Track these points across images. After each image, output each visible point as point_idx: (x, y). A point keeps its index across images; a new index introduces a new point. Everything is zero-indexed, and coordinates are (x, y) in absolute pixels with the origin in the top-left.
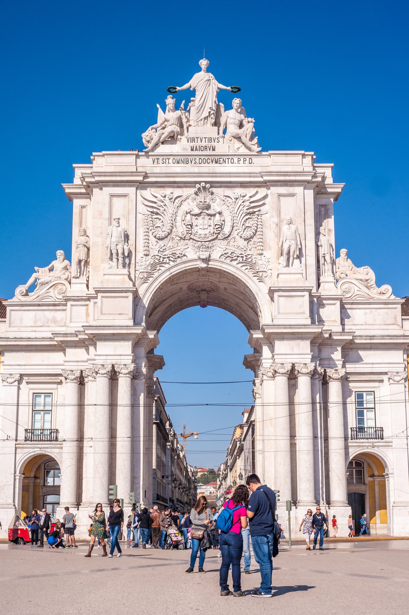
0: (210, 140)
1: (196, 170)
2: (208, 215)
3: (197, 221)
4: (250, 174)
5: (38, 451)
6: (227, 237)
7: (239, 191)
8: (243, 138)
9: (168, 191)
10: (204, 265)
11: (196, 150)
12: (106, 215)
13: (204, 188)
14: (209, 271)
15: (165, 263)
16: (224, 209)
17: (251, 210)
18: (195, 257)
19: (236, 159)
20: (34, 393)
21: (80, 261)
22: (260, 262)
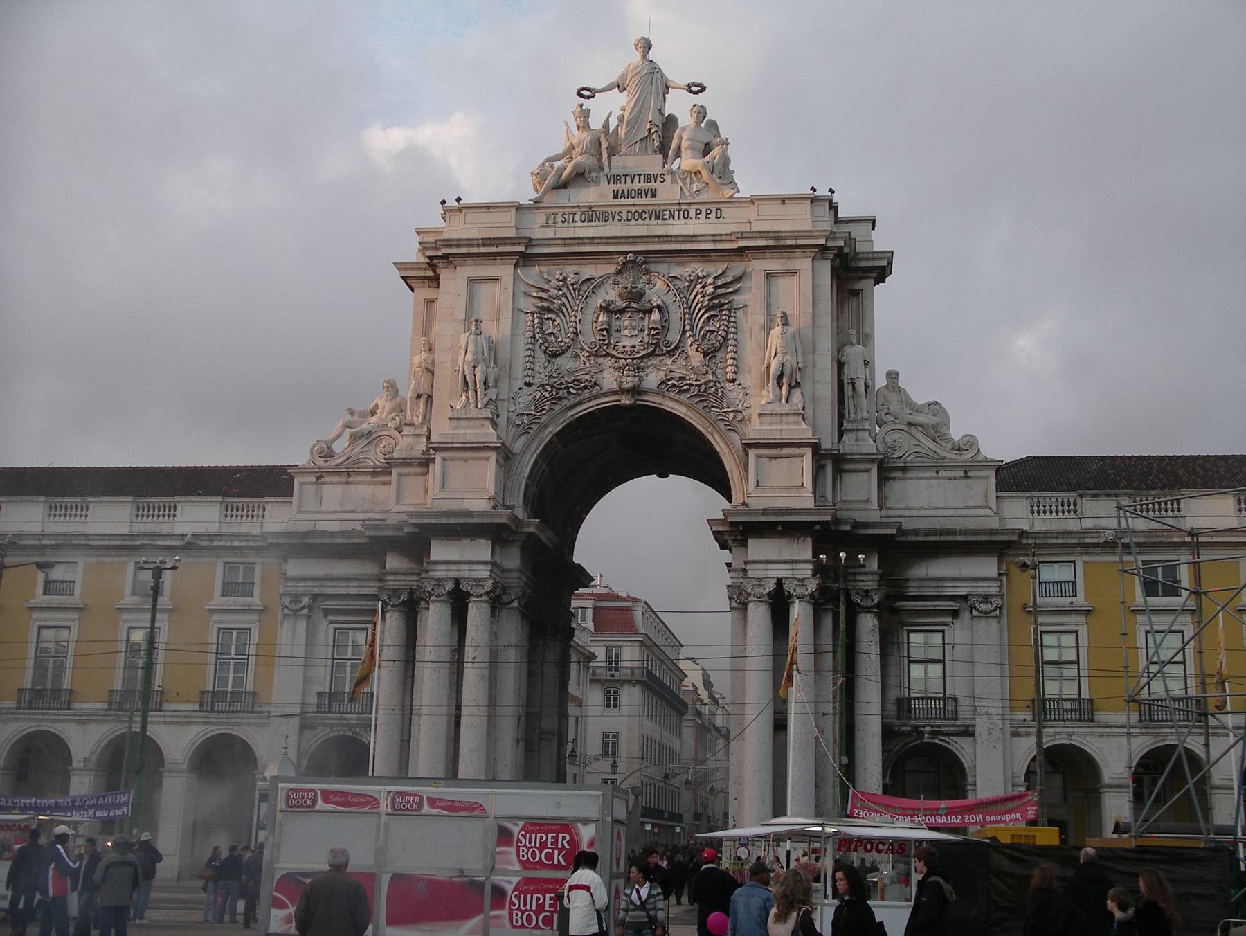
0: (648, 178)
2: (638, 311)
3: (618, 323)
4: (715, 237)
6: (673, 350)
7: (698, 268)
9: (570, 270)
10: (626, 401)
11: (623, 196)
13: (633, 262)
15: (560, 399)
16: (669, 299)
17: (716, 301)
18: (615, 386)
19: (692, 213)
20: (336, 629)
21: (419, 397)
22: (731, 395)
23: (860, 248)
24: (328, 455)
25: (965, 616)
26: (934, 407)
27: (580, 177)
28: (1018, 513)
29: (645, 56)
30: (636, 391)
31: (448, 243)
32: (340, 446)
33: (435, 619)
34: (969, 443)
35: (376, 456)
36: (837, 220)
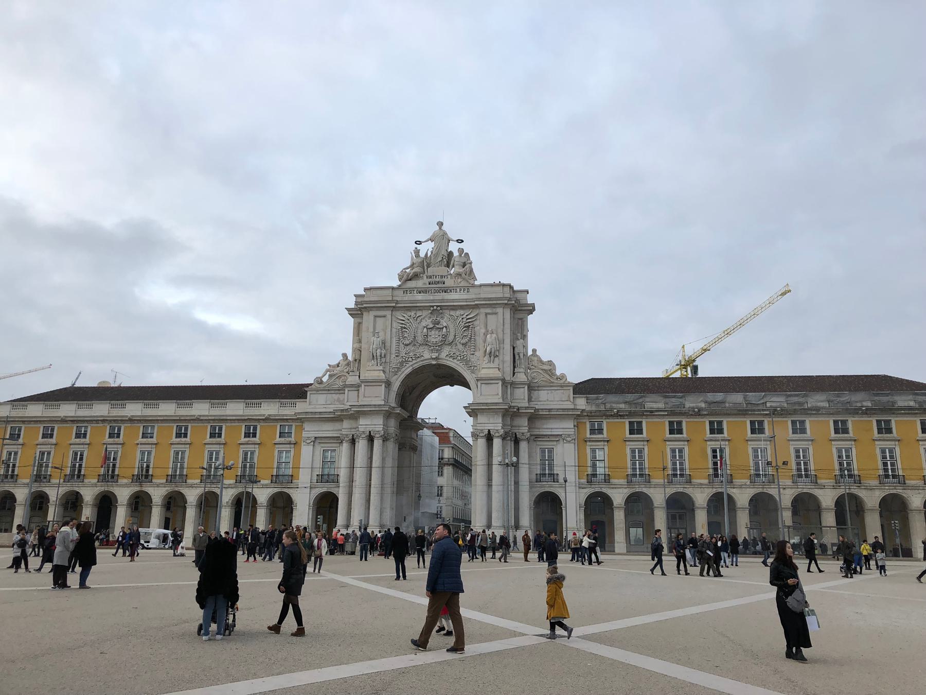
0: (442, 277)
1: (432, 298)
4: (466, 300)
5: (325, 490)
8: (463, 275)
9: (413, 314)
10: (434, 362)
12: (371, 330)
14: (440, 366)
23: (522, 302)
24: (321, 382)
25: (561, 441)
26: (550, 363)
27: (416, 276)
28: (581, 403)
29: (440, 228)
30: (437, 358)
31: (367, 302)
32: (325, 379)
33: (361, 445)
34: (563, 376)
35: (340, 383)
36: (514, 292)
